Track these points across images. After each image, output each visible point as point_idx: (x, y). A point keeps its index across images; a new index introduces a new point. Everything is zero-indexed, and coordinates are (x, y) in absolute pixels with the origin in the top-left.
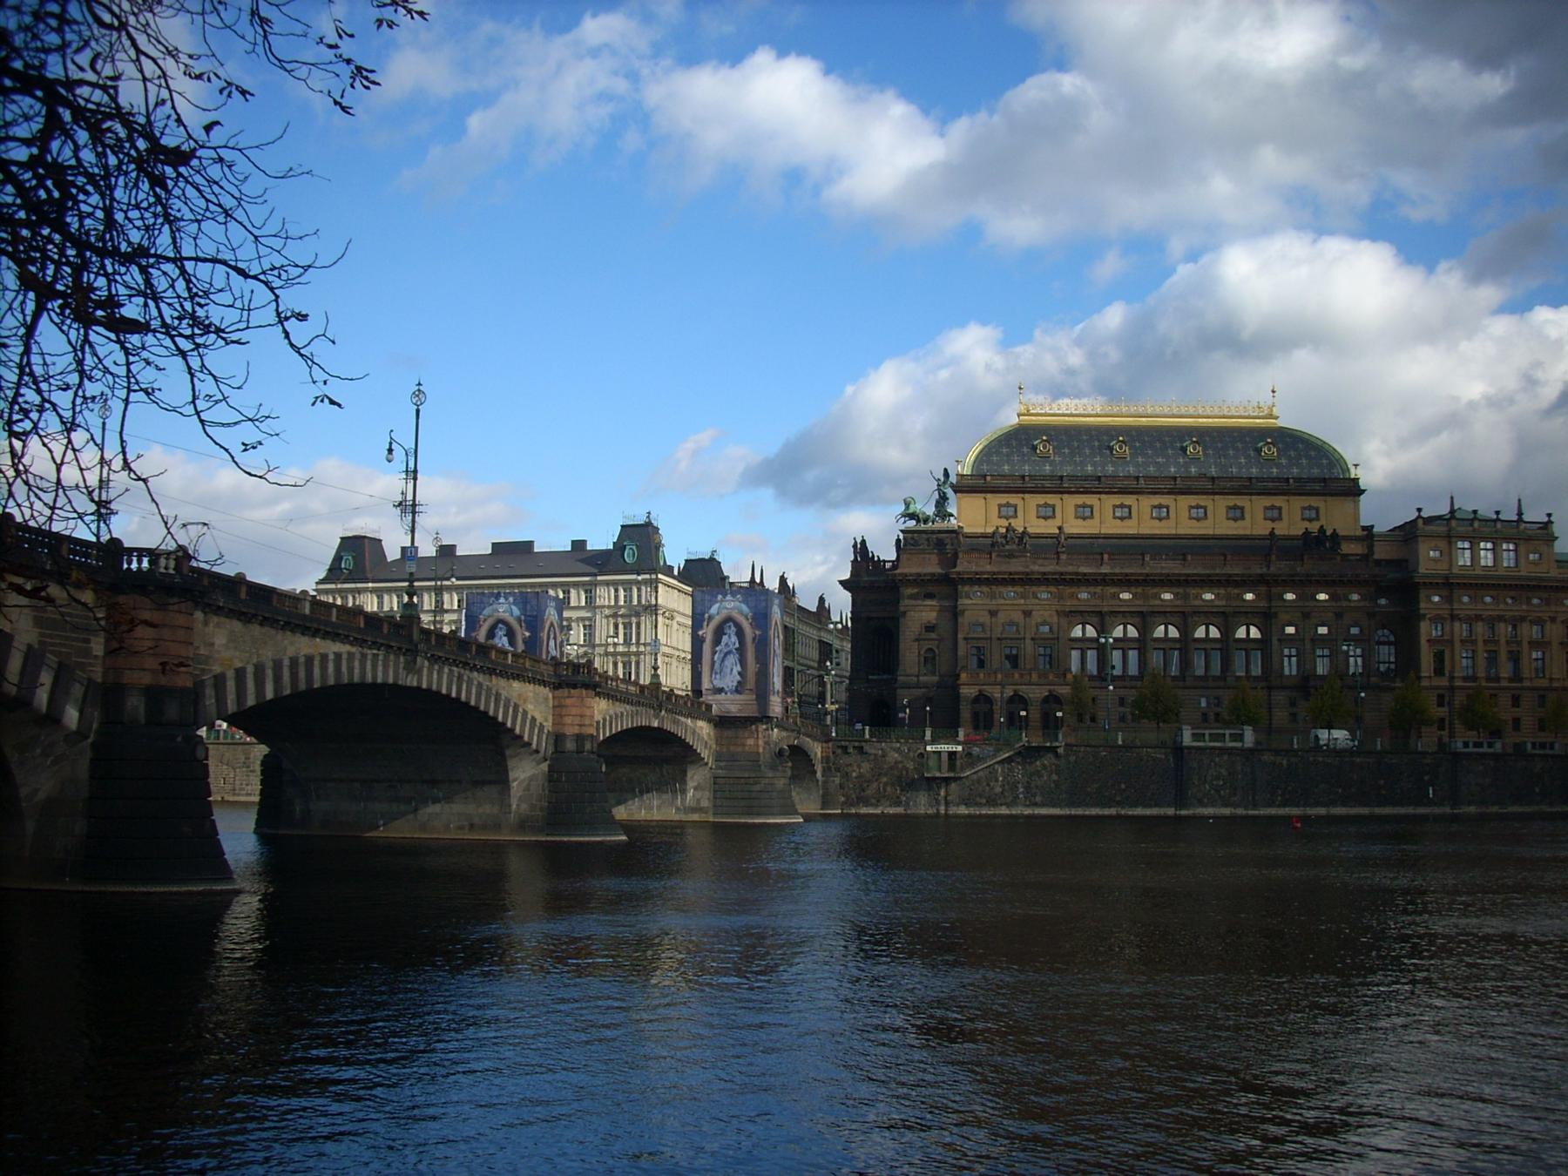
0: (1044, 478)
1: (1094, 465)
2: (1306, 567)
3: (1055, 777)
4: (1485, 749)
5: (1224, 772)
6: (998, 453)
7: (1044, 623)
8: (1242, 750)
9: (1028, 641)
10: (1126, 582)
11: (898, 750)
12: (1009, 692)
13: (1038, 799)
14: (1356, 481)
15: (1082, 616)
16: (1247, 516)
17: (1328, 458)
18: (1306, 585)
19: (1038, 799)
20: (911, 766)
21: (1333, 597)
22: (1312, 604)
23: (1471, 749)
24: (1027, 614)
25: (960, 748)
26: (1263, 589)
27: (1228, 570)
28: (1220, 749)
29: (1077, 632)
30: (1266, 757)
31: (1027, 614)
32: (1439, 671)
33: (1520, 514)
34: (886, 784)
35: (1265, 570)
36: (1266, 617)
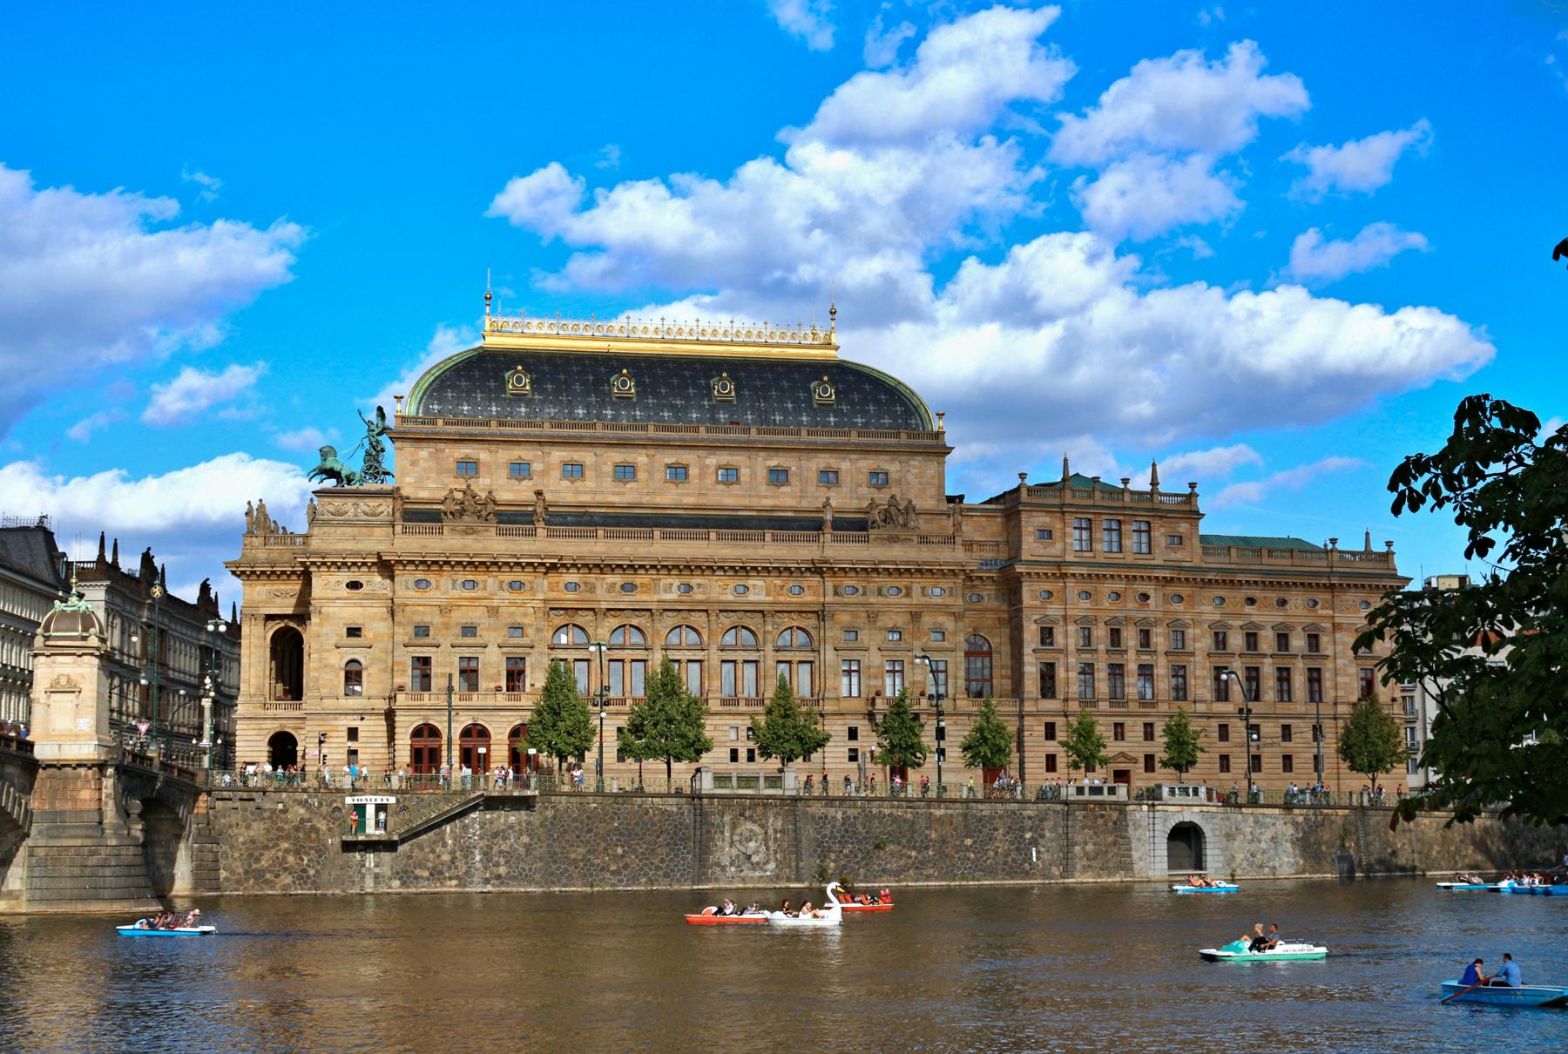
1: (587, 406)
3: (525, 839)
4: (1106, 797)
6: (453, 387)
8: (782, 799)
11: (304, 803)
14: (939, 435)
17: (903, 404)
19: (502, 870)
20: (322, 826)
23: (1087, 796)
25: (392, 800)
28: (752, 798)
30: (817, 809)
31: (493, 611)
33: (1154, 483)
34: (287, 851)
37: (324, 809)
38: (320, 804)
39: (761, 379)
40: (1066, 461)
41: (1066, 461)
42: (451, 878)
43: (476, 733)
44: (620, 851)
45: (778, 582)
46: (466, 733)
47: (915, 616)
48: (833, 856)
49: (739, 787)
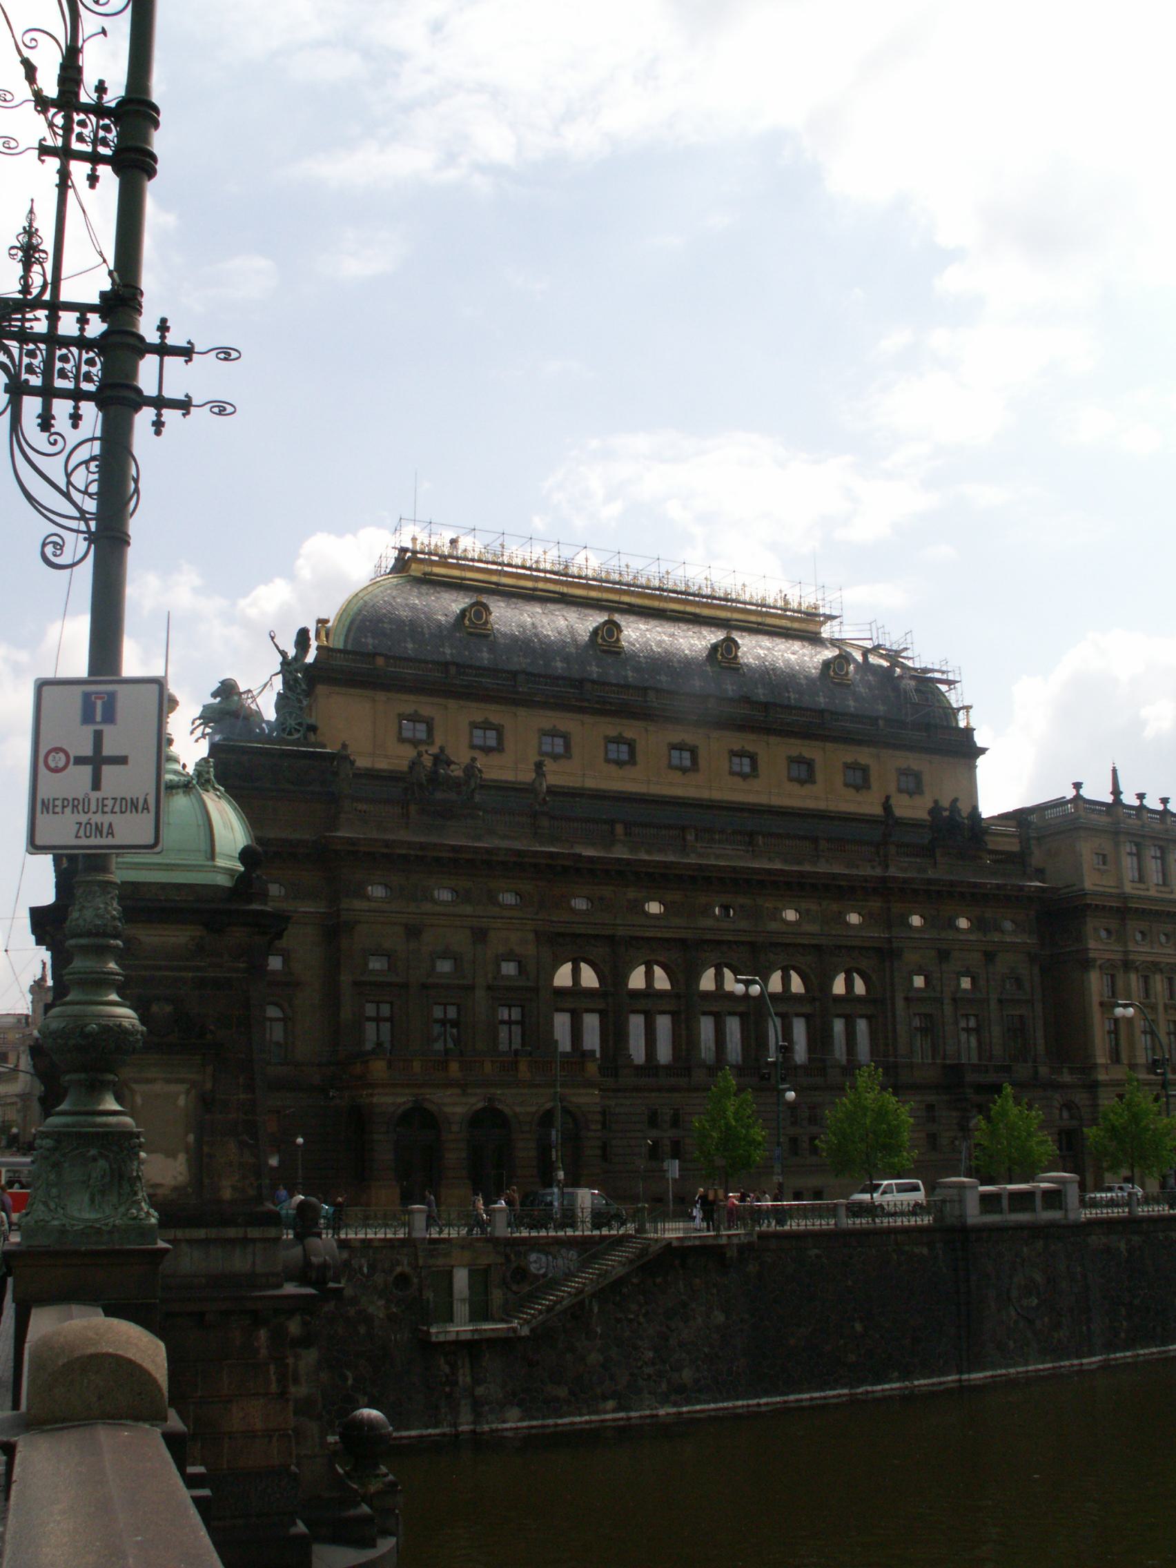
0: (482, 670)
2: (941, 871)
3: (719, 1317)
5: (1038, 1277)
7: (509, 956)
9: (480, 994)
10: (657, 879)
12: (476, 1102)
13: (687, 1375)
15: (573, 946)
16: (819, 776)
18: (937, 897)
19: (687, 1375)
21: (979, 924)
22: (950, 935)
24: (480, 935)
26: (876, 904)
27: (822, 868)
29: (563, 976)
31: (480, 935)
32: (1116, 1057)
35: (878, 872)
36: (880, 958)
37: (379, 1279)
38: (372, 1267)
39: (760, 647)
40: (1114, 771)
41: (1114, 771)
42: (605, 1398)
43: (490, 1120)
44: (858, 1327)
45: (835, 907)
46: (476, 1120)
47: (989, 957)
48: (1123, 1312)
49: (1013, 1209)
